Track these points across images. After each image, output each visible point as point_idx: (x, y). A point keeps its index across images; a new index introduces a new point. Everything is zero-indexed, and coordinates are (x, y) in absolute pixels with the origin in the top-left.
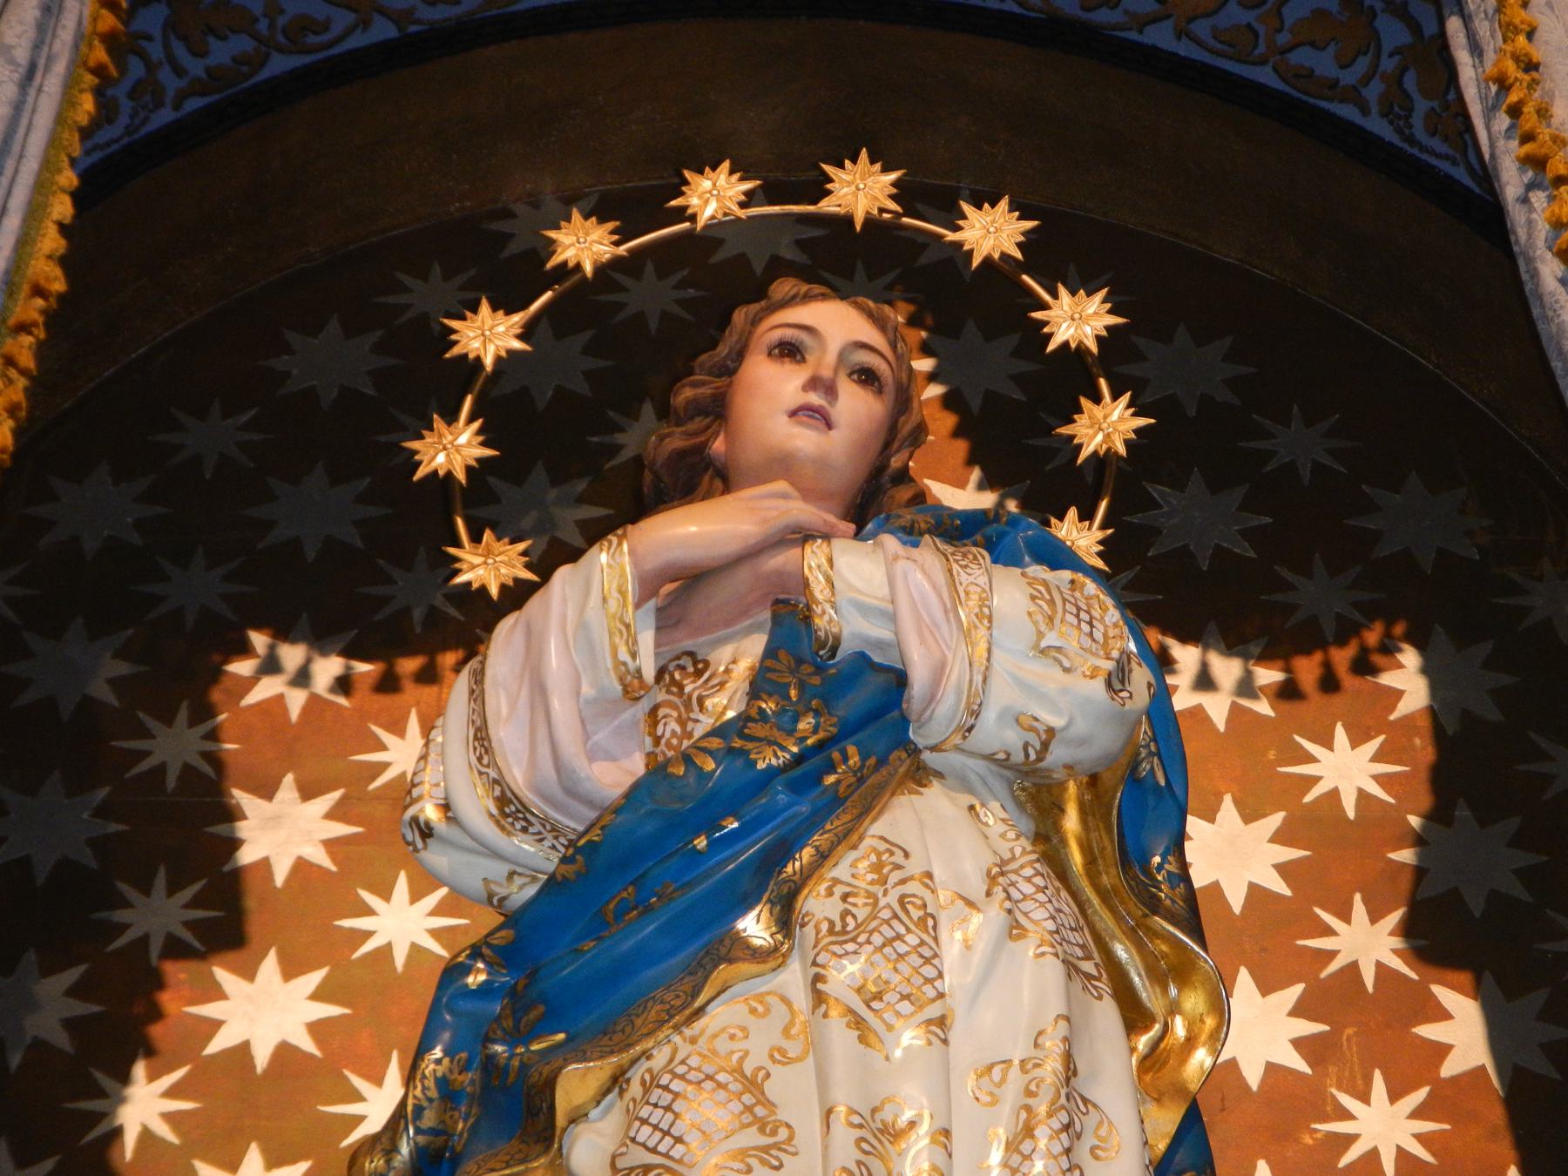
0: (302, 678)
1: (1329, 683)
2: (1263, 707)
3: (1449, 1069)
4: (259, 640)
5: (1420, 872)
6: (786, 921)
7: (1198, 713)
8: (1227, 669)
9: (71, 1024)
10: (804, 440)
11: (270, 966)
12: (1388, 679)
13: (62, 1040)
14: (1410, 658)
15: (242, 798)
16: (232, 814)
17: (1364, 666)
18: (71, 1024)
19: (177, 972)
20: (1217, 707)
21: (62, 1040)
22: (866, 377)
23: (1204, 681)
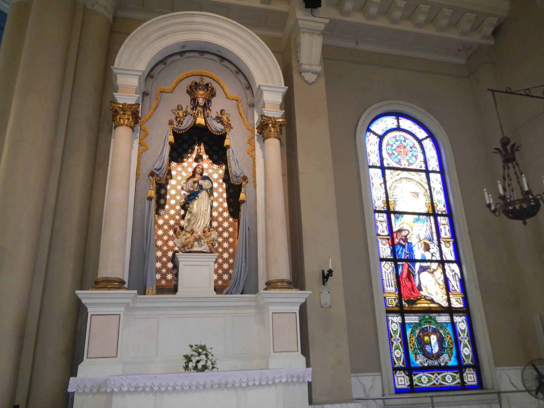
0: (174, 164)
1: (220, 167)
2: (217, 168)
3: (224, 187)
4: (172, 162)
5: (223, 177)
6: (198, 198)
7: (214, 168)
8: (216, 166)
9: (165, 183)
10: (199, 172)
11: (173, 180)
12: (223, 167)
13: (165, 183)
14: (224, 166)
15: (172, 171)
16: (171, 172)
17: (222, 166)
18: (165, 183)
19: (169, 180)
20: (215, 168)
21: (165, 183)
22: (202, 169)
23: (215, 167)
